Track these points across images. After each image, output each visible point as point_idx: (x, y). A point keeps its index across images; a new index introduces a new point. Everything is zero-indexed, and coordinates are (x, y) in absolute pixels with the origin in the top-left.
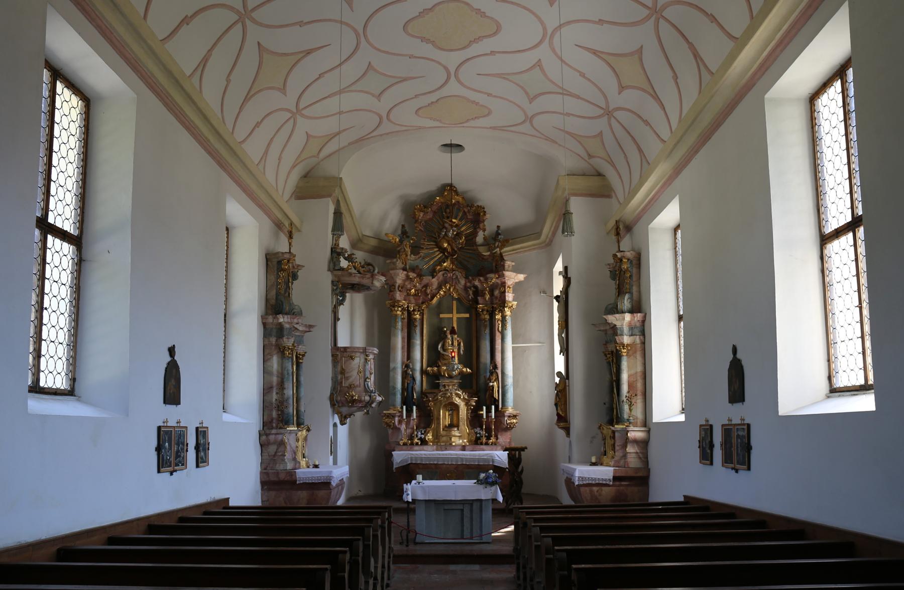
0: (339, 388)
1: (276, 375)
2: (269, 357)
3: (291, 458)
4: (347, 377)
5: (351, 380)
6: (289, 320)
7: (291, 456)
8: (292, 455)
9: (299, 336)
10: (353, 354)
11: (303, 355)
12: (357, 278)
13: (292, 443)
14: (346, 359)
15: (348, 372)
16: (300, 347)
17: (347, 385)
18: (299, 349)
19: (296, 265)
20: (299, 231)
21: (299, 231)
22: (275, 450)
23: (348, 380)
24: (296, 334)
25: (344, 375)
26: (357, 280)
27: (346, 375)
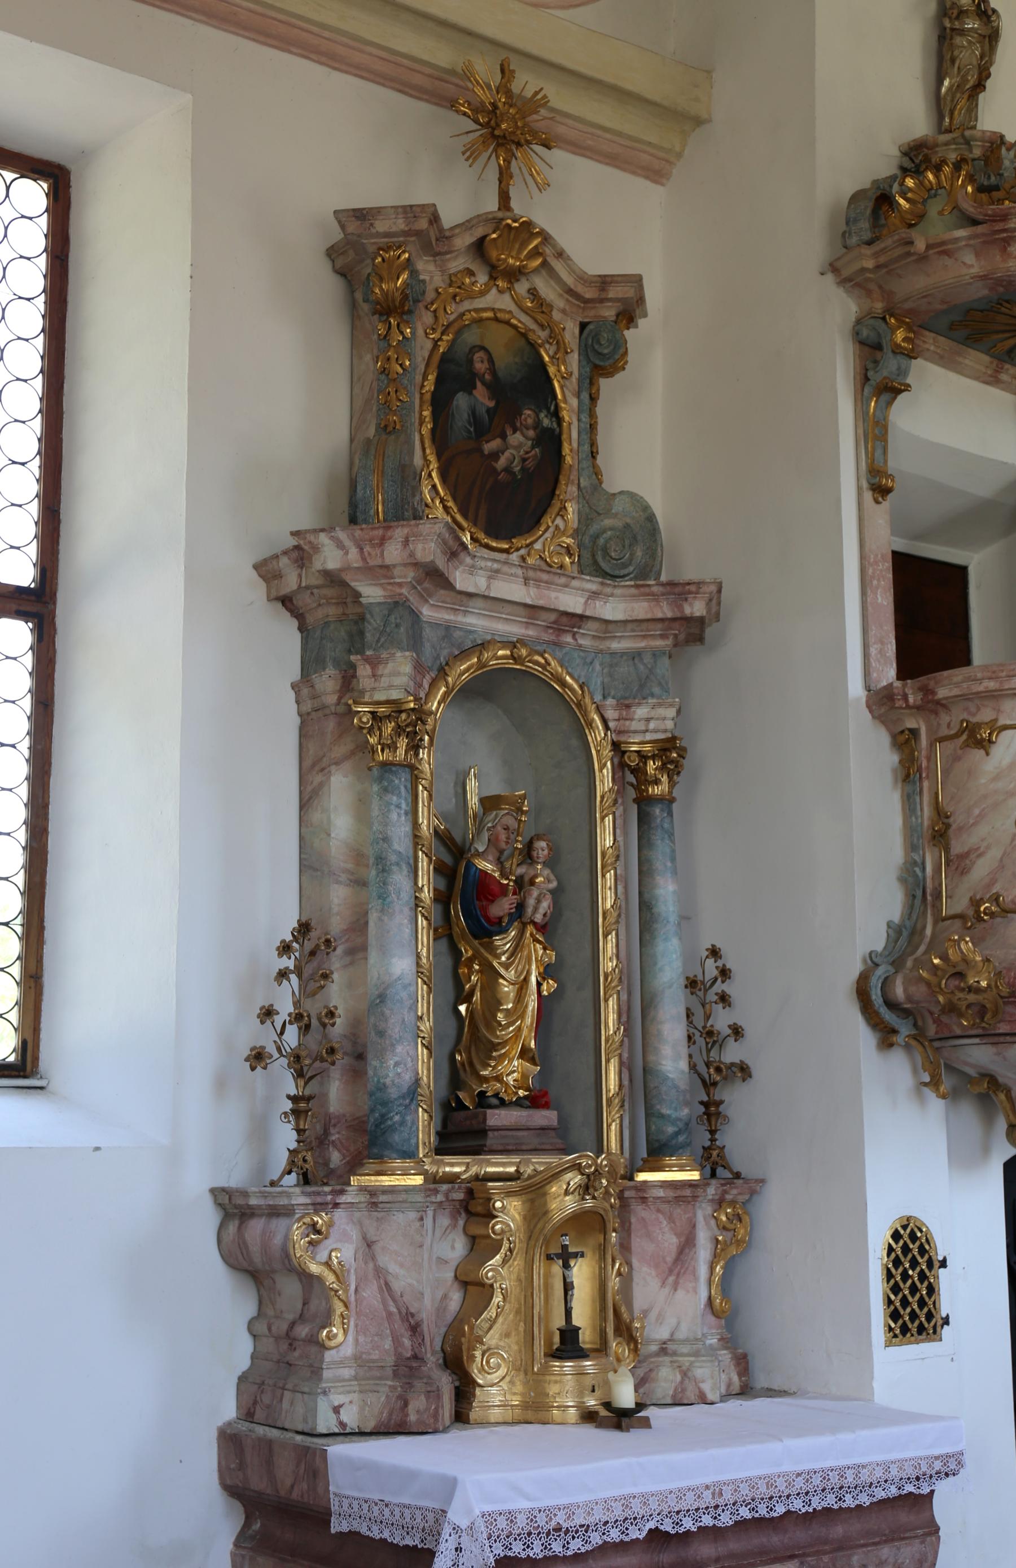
0: (929, 931)
1: (343, 877)
2: (318, 779)
3: (390, 1360)
4: (964, 856)
5: (981, 870)
6: (353, 553)
7: (388, 1344)
8: (396, 1341)
9: (635, 656)
10: (985, 715)
11: (673, 768)
12: (969, 258)
13: (393, 1268)
14: (950, 746)
15: (960, 829)
16: (641, 712)
17: (961, 904)
18: (634, 725)
19: (583, 278)
20: (698, 122)
21: (698, 122)
22: (299, 1306)
23: (964, 872)
24: (615, 645)
25: (947, 850)
26: (974, 271)
27: (957, 847)
